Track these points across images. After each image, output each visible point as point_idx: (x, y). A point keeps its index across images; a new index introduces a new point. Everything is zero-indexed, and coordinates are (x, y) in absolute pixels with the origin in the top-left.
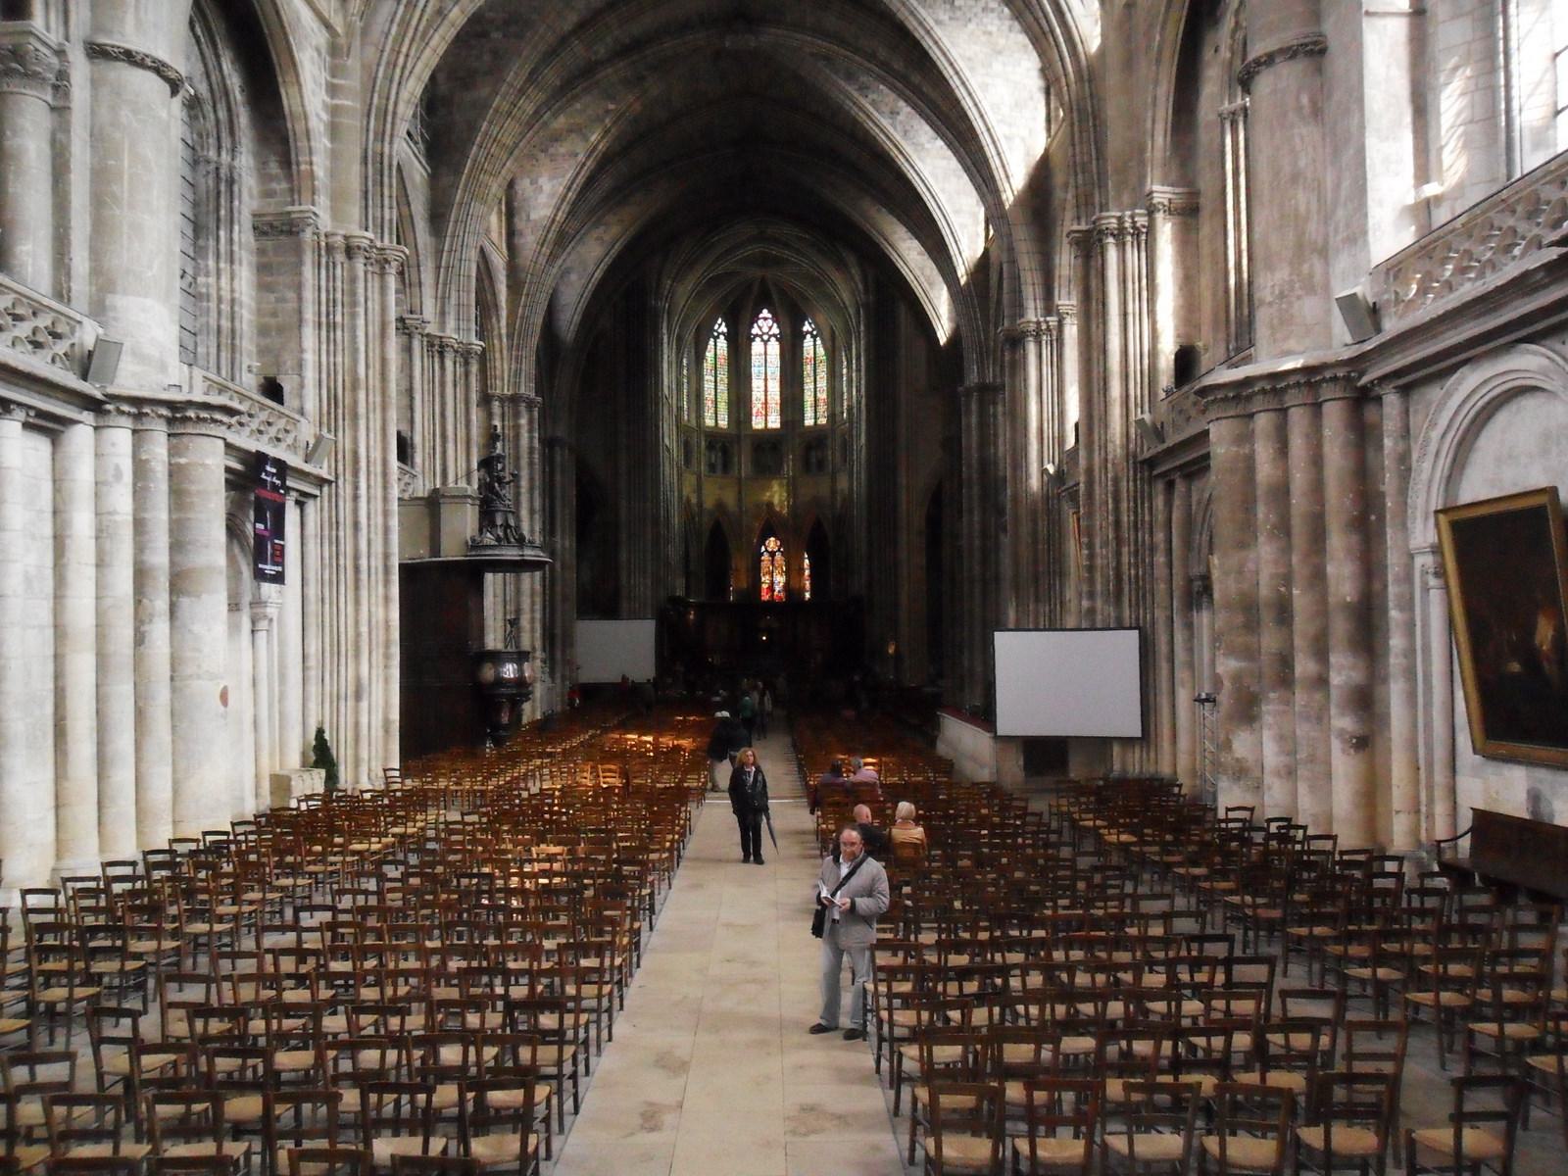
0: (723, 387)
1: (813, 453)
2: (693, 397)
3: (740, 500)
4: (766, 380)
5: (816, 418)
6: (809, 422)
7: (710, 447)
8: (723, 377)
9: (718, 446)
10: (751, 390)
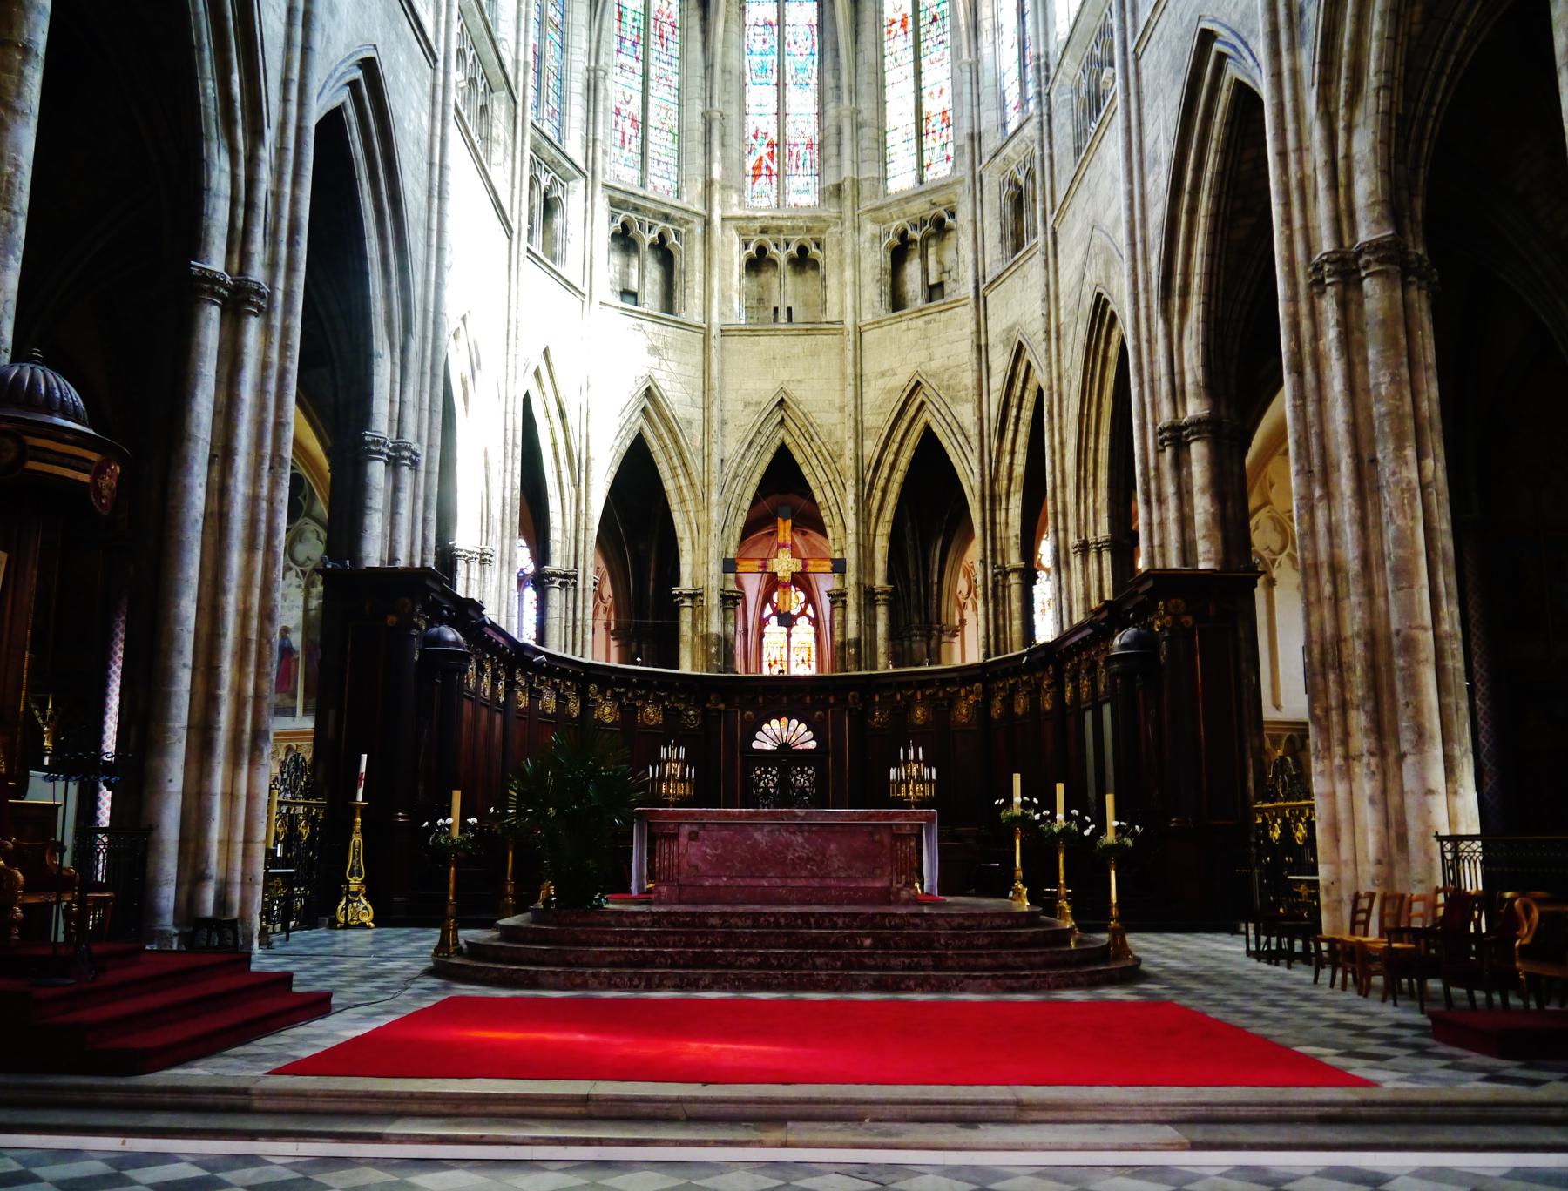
0: (662, 95)
1: (912, 270)
2: (577, 86)
3: (706, 390)
4: (781, 86)
5: (920, 166)
6: (901, 178)
7: (624, 240)
8: (664, 68)
9: (649, 238)
10: (743, 113)
